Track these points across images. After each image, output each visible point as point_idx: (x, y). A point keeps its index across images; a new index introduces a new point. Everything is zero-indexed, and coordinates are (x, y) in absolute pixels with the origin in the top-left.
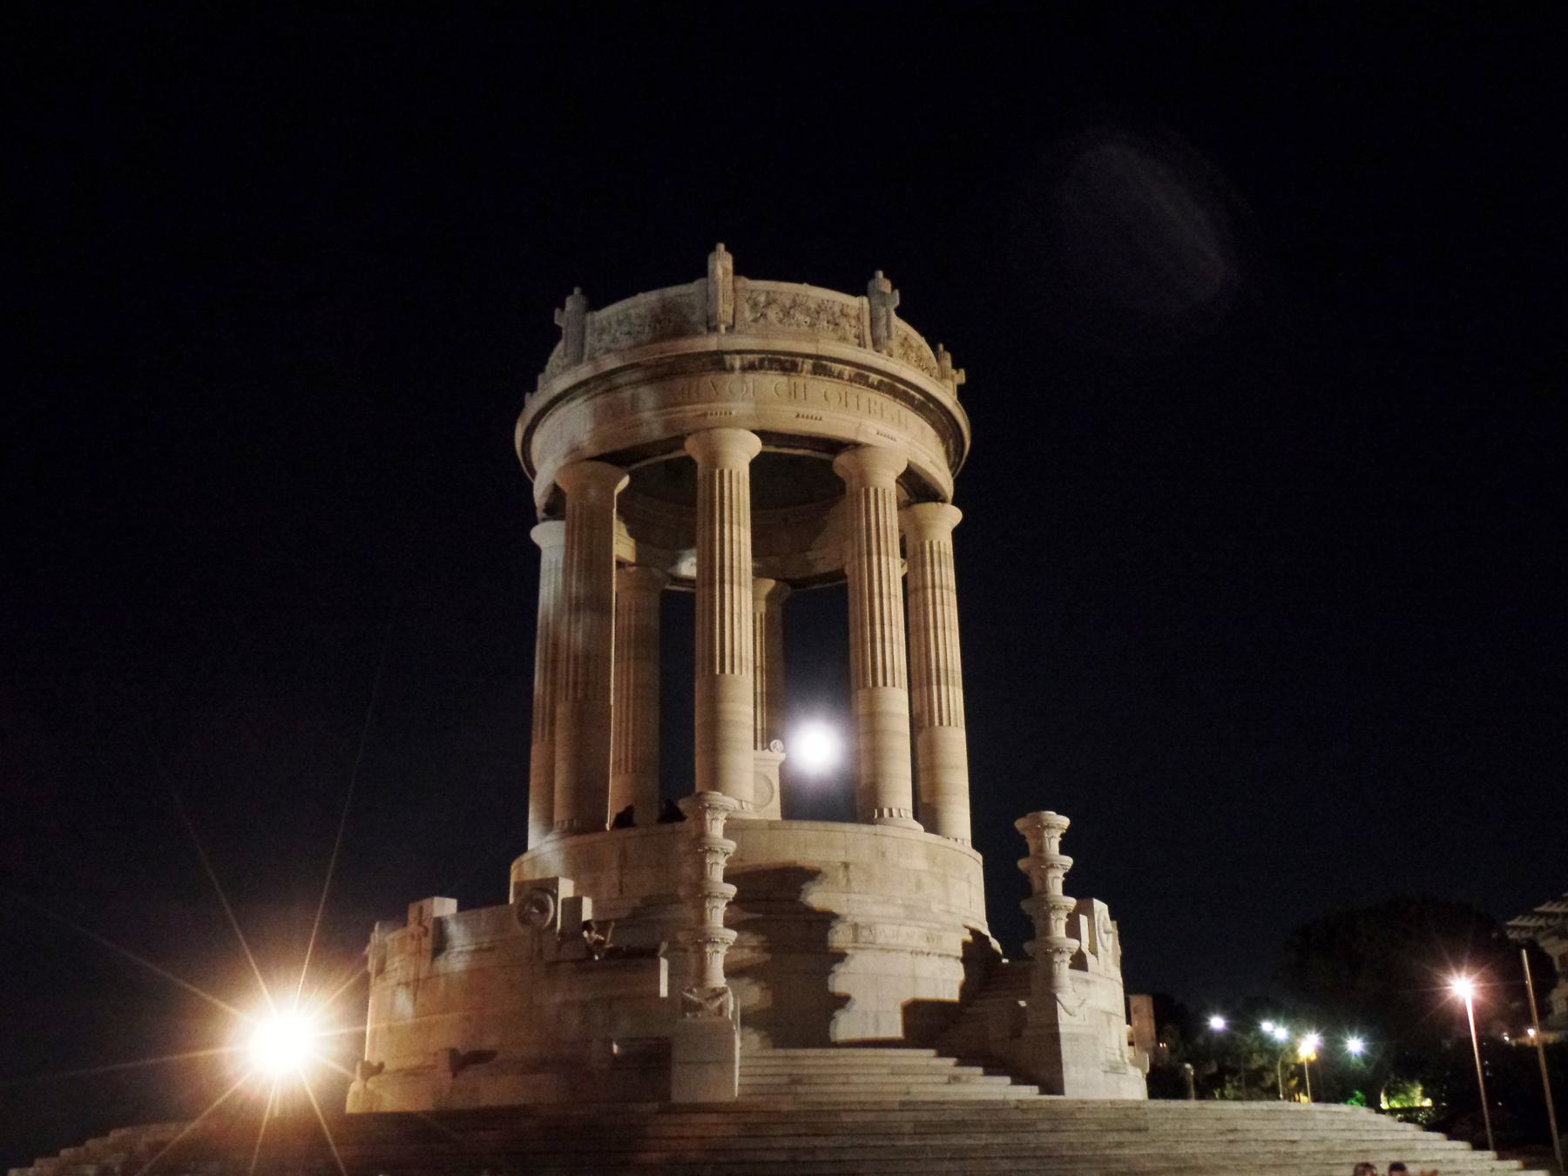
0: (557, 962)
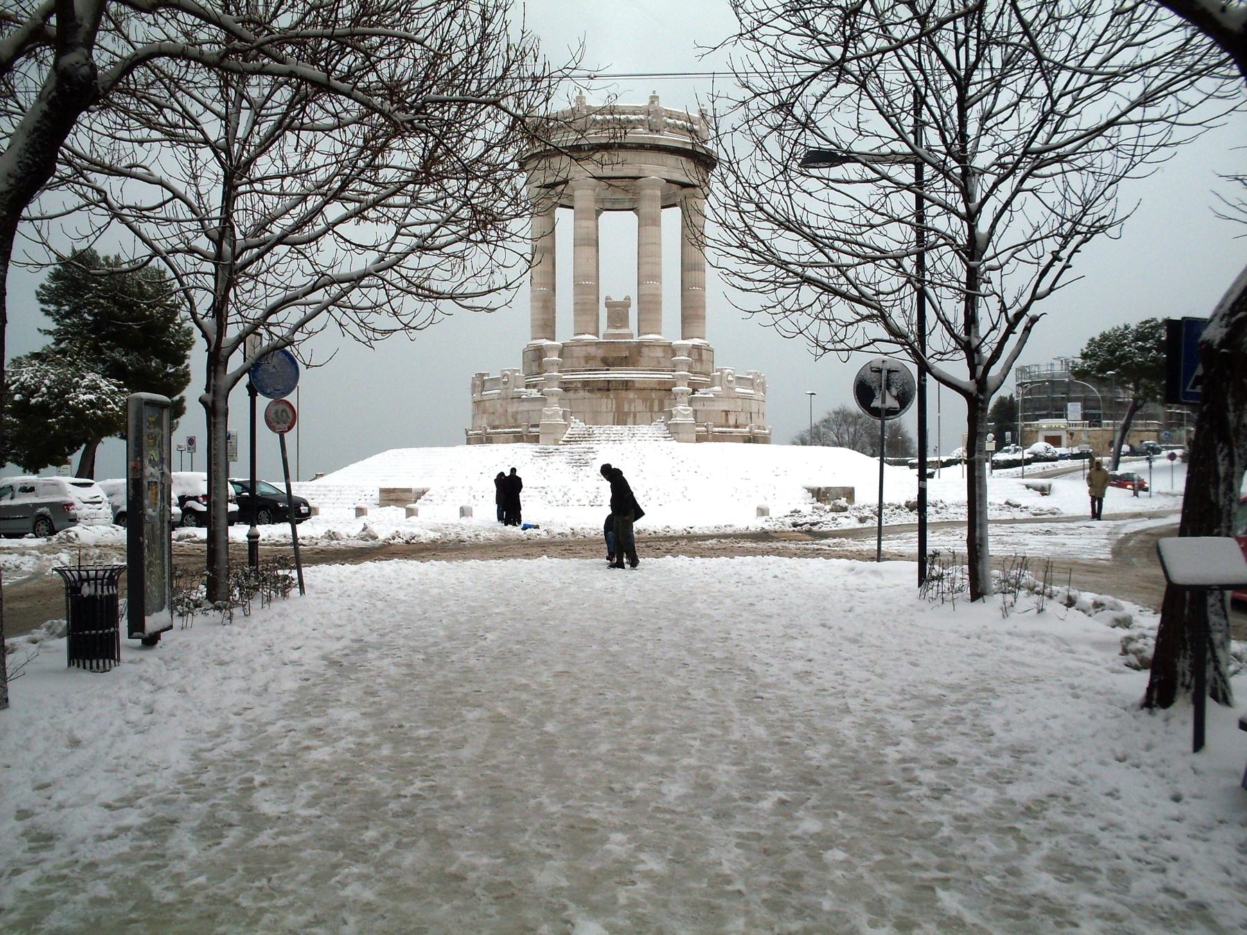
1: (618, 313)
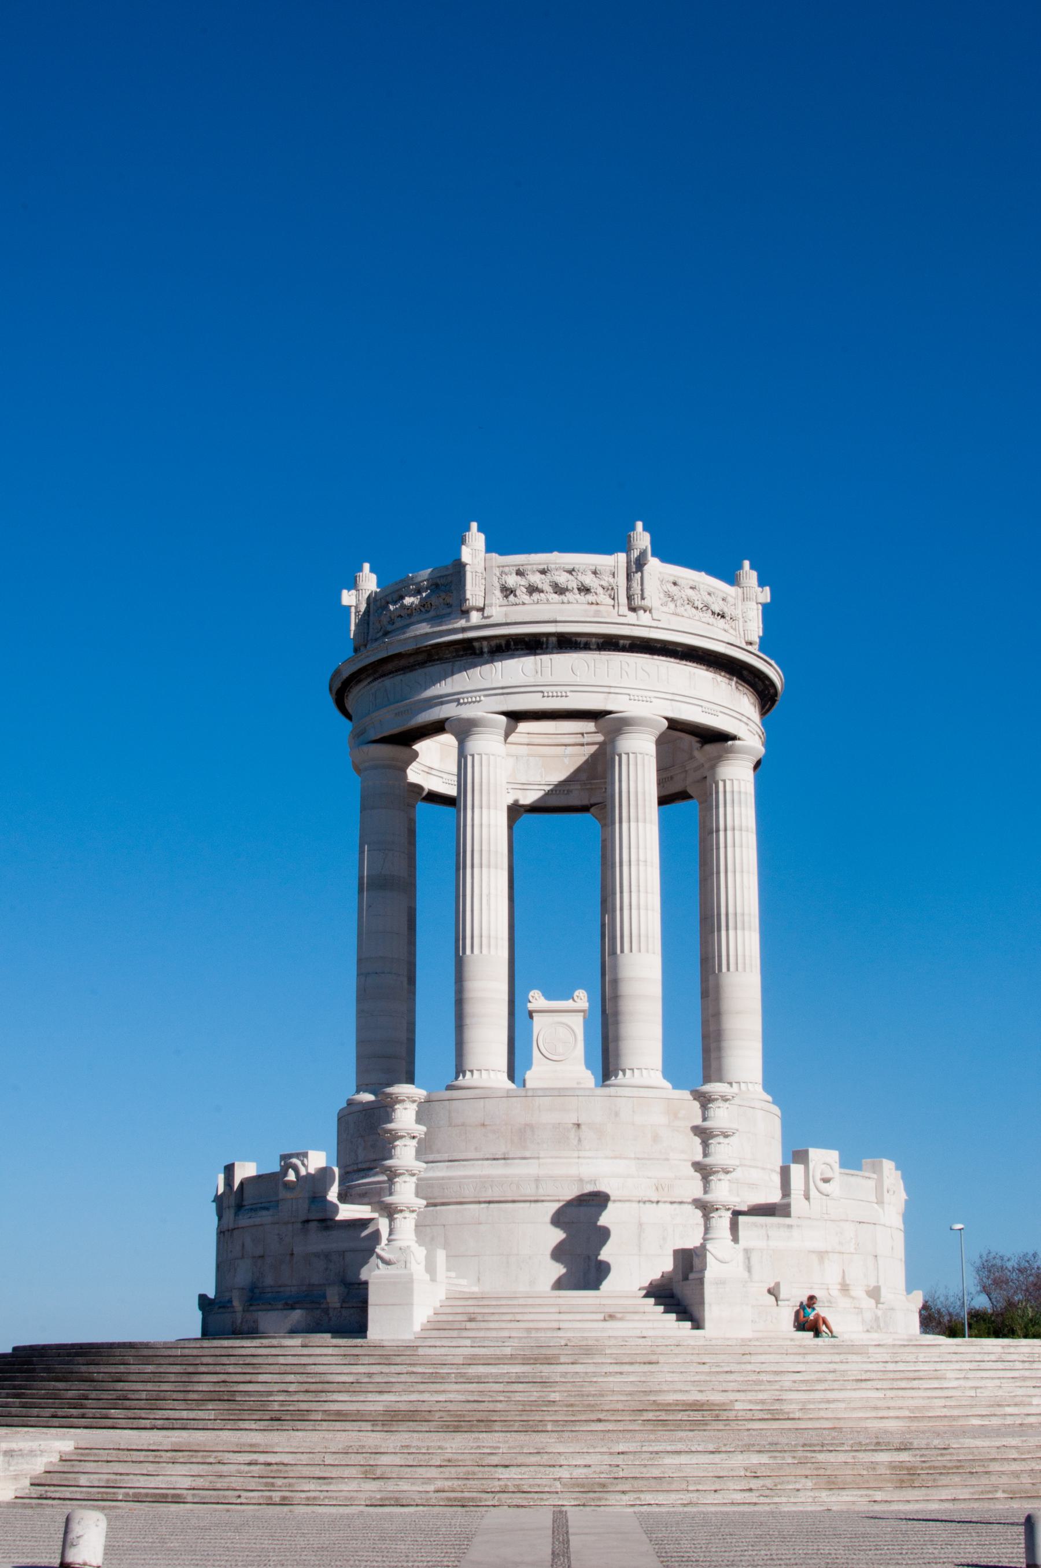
0: (307, 1221)
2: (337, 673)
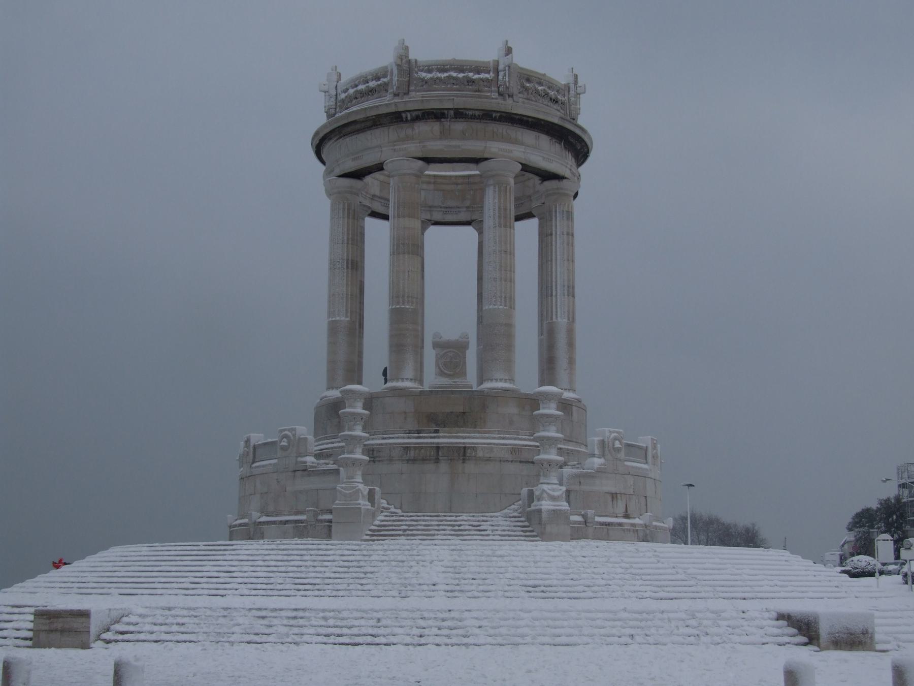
0: (295, 471)
1: (452, 355)
2: (317, 133)
